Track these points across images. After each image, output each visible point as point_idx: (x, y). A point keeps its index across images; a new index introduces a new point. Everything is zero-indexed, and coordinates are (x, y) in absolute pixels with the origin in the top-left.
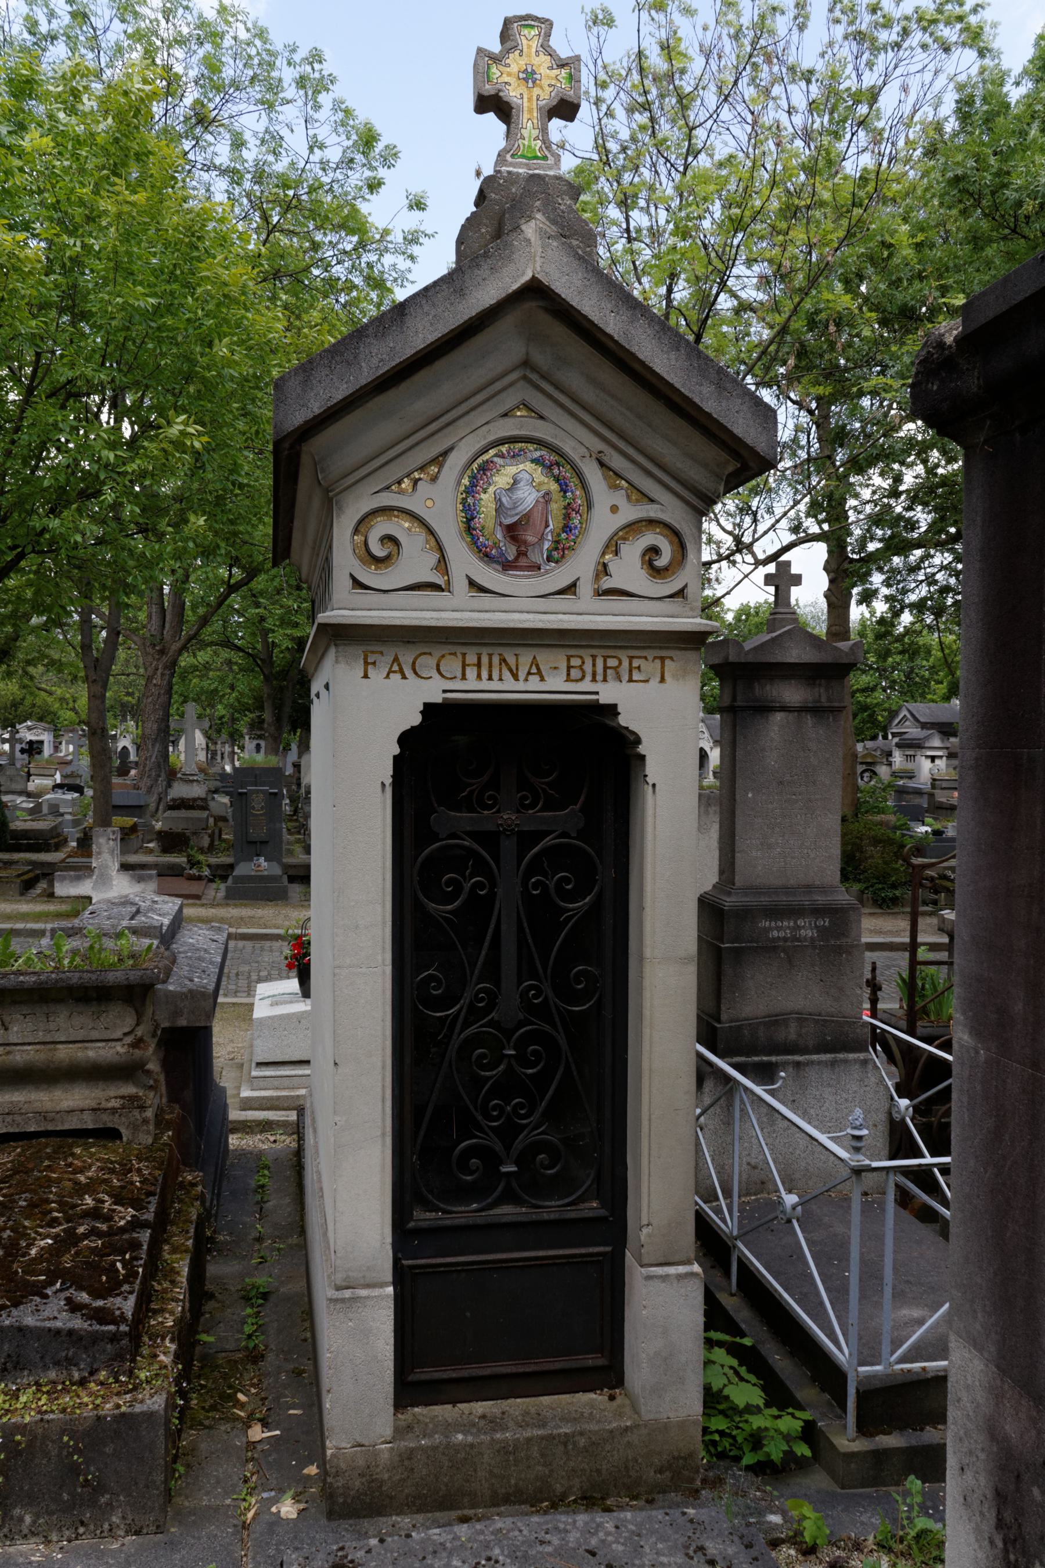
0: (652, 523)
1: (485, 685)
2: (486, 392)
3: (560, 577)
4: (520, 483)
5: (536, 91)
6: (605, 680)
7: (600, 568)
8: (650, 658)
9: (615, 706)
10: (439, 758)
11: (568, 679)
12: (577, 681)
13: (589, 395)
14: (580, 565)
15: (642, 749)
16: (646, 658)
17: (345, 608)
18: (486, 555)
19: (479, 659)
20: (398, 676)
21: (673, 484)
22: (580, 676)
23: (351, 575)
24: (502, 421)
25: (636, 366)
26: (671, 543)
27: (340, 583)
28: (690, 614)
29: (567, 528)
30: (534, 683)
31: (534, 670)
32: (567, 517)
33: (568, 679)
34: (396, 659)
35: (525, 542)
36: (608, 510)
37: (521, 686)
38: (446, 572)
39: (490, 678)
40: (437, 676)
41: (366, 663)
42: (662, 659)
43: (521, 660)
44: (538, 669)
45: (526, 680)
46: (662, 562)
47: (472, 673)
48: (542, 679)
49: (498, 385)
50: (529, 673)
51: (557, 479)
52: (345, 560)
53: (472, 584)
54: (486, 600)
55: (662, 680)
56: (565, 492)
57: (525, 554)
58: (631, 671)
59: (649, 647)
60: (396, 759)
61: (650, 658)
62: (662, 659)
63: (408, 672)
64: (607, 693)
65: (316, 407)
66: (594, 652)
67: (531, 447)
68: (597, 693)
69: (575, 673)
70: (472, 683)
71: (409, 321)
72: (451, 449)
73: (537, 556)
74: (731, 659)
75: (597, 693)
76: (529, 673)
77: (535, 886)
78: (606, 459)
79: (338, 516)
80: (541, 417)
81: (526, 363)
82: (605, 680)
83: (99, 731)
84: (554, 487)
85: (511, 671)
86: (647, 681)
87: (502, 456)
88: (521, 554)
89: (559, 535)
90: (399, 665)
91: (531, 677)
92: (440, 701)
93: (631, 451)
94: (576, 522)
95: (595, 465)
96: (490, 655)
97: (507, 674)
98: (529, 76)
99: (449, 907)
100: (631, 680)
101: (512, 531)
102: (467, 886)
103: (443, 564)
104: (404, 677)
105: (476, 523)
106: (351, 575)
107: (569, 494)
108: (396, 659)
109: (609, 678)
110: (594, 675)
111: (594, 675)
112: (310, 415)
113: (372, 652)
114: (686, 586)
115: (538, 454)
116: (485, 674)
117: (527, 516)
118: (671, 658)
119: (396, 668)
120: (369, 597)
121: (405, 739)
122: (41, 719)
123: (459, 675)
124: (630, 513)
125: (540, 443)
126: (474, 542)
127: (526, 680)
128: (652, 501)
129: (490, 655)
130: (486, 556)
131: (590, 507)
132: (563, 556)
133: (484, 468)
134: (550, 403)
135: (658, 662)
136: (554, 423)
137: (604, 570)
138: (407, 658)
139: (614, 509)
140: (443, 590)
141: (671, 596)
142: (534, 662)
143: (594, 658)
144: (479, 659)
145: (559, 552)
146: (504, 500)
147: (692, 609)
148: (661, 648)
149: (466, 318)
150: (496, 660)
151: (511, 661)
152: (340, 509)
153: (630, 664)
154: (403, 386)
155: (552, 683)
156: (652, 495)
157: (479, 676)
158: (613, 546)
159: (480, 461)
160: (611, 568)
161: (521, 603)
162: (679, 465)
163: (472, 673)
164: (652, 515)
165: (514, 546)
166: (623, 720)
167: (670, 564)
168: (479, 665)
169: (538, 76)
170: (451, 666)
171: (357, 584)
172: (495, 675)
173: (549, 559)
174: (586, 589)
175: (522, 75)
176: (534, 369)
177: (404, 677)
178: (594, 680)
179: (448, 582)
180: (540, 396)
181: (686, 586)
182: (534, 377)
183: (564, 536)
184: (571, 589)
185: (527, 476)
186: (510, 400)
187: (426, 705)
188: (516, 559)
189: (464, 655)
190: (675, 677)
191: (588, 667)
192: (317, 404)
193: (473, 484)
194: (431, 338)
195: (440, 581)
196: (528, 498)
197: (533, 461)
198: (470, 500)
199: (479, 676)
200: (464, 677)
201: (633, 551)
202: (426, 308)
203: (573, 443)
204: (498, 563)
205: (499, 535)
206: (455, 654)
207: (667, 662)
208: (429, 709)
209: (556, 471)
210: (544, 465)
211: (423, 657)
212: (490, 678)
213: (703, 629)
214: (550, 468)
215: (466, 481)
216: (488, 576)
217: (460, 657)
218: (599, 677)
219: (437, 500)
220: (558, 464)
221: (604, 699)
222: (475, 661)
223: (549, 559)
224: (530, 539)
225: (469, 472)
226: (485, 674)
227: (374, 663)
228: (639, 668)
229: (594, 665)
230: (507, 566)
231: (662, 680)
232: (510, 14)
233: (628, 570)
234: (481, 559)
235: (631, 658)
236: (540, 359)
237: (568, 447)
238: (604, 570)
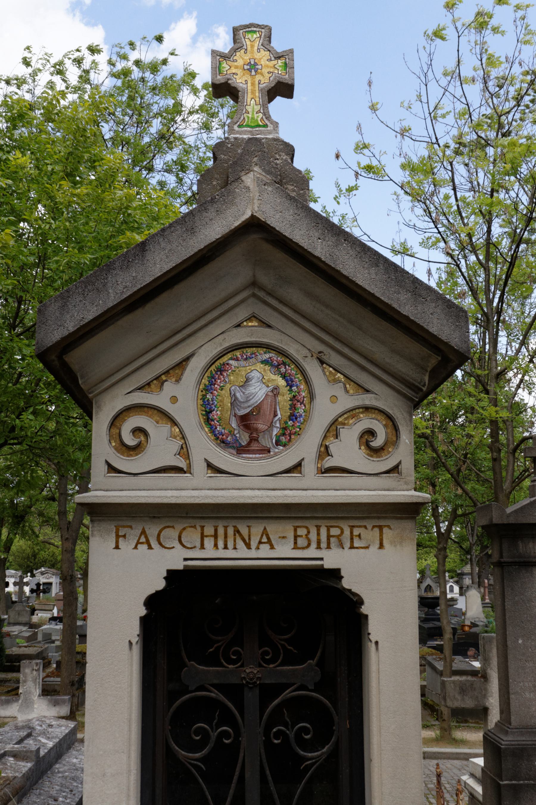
0: (367, 409)
2: (221, 309)
3: (286, 458)
4: (257, 383)
5: (258, 77)
6: (329, 547)
7: (323, 449)
8: (369, 527)
9: (338, 571)
10: (181, 617)
11: (296, 547)
12: (303, 548)
13: (306, 305)
14: (306, 447)
15: (364, 610)
16: (365, 527)
17: (103, 490)
18: (223, 442)
19: (216, 531)
20: (145, 546)
21: (385, 377)
22: (306, 544)
23: (107, 462)
24: (235, 331)
25: (344, 281)
26: (385, 426)
27: (98, 469)
28: (405, 487)
29: (293, 417)
30: (265, 551)
31: (265, 540)
32: (293, 407)
33: (296, 547)
34: (143, 532)
35: (256, 430)
36: (330, 398)
37: (253, 553)
38: (187, 457)
39: (226, 547)
41: (118, 536)
42: (381, 528)
43: (253, 530)
45: (258, 548)
46: (378, 442)
47: (209, 543)
48: (272, 547)
49: (232, 303)
50: (260, 542)
51: (284, 377)
52: (102, 449)
53: (210, 466)
54: (222, 480)
55: (381, 546)
56: (291, 387)
57: (257, 440)
58: (352, 539)
59: (368, 518)
60: (144, 620)
61: (369, 527)
62: (381, 528)
63: (154, 543)
64: (331, 559)
65: (71, 326)
66: (318, 522)
67: (261, 351)
68: (322, 559)
69: (301, 542)
70: (209, 551)
71: (149, 256)
72: (192, 355)
73: (266, 441)
74: (495, 521)
75: (322, 559)
76: (260, 542)
77: (277, 735)
78: (325, 358)
79: (97, 413)
80: (269, 326)
81: (254, 284)
82: (329, 547)
83: (69, 578)
84: (282, 382)
85: (244, 540)
86: (367, 547)
87: (237, 359)
88: (252, 439)
89: (286, 423)
90: (146, 537)
91: (262, 546)
92: (180, 567)
93: (346, 351)
94: (301, 411)
95: (316, 363)
96: (226, 528)
97: (240, 544)
98: (252, 67)
99: (197, 755)
100: (352, 547)
101: (245, 421)
102: (214, 735)
103: (184, 451)
104: (150, 547)
105: (216, 414)
106: (107, 462)
107: (294, 388)
108: (143, 532)
109: (332, 545)
110: (319, 542)
111: (319, 542)
112: (66, 333)
113: (124, 527)
114: (400, 463)
116: (221, 544)
117: (258, 408)
118: (389, 527)
119: (143, 539)
120: (116, 480)
121: (151, 602)
122: (53, 566)
123: (198, 544)
125: (268, 347)
126: (213, 430)
127: (258, 548)
128: (367, 391)
129: (226, 528)
130: (222, 442)
131: (312, 396)
132: (290, 441)
133: (220, 370)
134: (275, 314)
135: (377, 530)
136: (280, 331)
137: (325, 452)
138: (152, 530)
139: (334, 399)
140: (185, 472)
141: (388, 472)
142: (265, 532)
143: (318, 527)
144: (216, 531)
145: (286, 438)
146: (238, 395)
147: (406, 483)
148: (379, 518)
149: (196, 250)
150: (231, 531)
151: (244, 531)
152: (99, 407)
153: (352, 533)
154: (149, 306)
155: (280, 550)
156: (366, 386)
157: (216, 545)
158: (333, 429)
159: (217, 364)
160: (333, 449)
161: (253, 482)
162: (387, 360)
163: (209, 543)
164: (368, 403)
165: (247, 433)
166: (346, 584)
167: (386, 443)
168: (216, 536)
169: (260, 67)
170: (192, 537)
171: (112, 469)
172: (230, 544)
173: (278, 443)
174: (310, 468)
175: (246, 67)
176: (262, 288)
177: (150, 547)
178: (319, 547)
179: (189, 466)
180: (270, 311)
181: (400, 463)
182: (261, 294)
183: (290, 423)
184: (297, 468)
185: (258, 375)
186: (242, 313)
187: (168, 571)
188: (249, 444)
189: (202, 527)
190: (393, 543)
191: (313, 536)
192: (72, 324)
193: (212, 384)
194: (167, 267)
195: (182, 463)
196: (258, 392)
197: (262, 362)
198: (209, 396)
199: (216, 545)
200: (202, 547)
201: (350, 435)
202: (163, 245)
203: (296, 346)
204: (233, 448)
205: (234, 425)
206: (194, 527)
207: (385, 530)
208: (172, 576)
209: (283, 370)
210: (272, 365)
211: (167, 530)
212: (226, 547)
213: (415, 500)
214: (277, 367)
215: (205, 381)
216: (224, 459)
217: (199, 529)
218: (324, 545)
219: (181, 397)
220: (284, 364)
221: (328, 564)
222: (212, 532)
223: (278, 443)
224: (261, 426)
226: (221, 544)
227: (124, 536)
228: (359, 536)
229: (318, 534)
231: (381, 546)
232: (237, 24)
233: (347, 450)
234: (219, 445)
235: (352, 527)
236: (264, 279)
237: (292, 349)
238: (325, 452)
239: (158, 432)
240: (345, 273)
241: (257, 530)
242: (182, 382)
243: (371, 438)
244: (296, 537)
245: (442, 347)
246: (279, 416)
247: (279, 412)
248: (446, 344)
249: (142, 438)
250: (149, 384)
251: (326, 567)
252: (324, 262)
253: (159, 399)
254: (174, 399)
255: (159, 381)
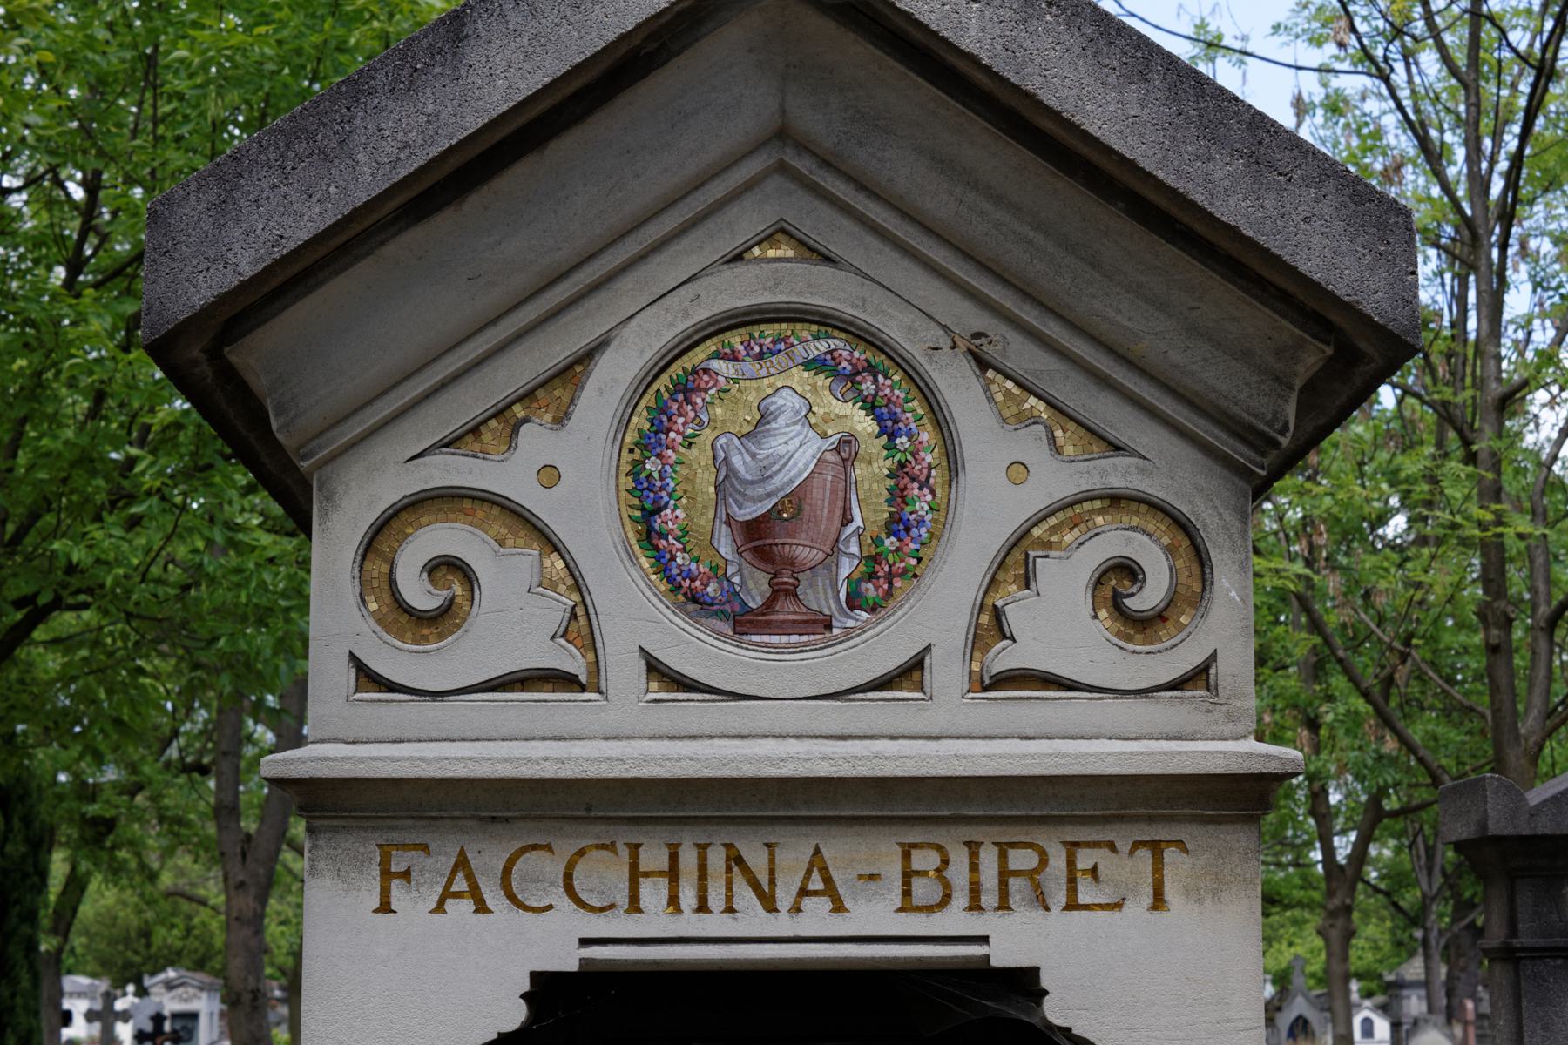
0: (1115, 500)
1: (690, 924)
2: (683, 209)
3: (883, 646)
4: (794, 425)
6: (1004, 906)
7: (985, 619)
8: (1124, 846)
9: (1035, 971)
12: (929, 909)
13: (938, 199)
14: (936, 613)
16: (1112, 846)
17: (347, 740)
18: (693, 598)
19: (674, 858)
20: (467, 905)
21: (1167, 405)
22: (937, 897)
23: (353, 657)
24: (727, 273)
25: (1047, 124)
26: (1170, 551)
27: (327, 676)
28: (1228, 728)
29: (898, 525)
30: (817, 917)
31: (816, 884)
32: (898, 496)
34: (462, 864)
35: (791, 563)
36: (1005, 471)
37: (782, 924)
38: (590, 644)
39: (703, 907)
40: (566, 904)
41: (387, 875)
42: (1156, 848)
43: (783, 858)
44: (828, 880)
45: (796, 909)
46: (1147, 599)
47: (653, 893)
48: (839, 907)
49: (717, 190)
50: (804, 892)
51: (871, 407)
52: (338, 621)
53: (655, 669)
54: (691, 711)
55: (1158, 902)
56: (892, 436)
57: (792, 593)
58: (1072, 881)
59: (1120, 819)
61: (1124, 846)
62: (1156, 848)
63: (493, 896)
64: (1011, 940)
65: (246, 262)
66: (973, 833)
67: (804, 331)
68: (984, 940)
69: (924, 890)
70: (655, 919)
71: (473, 53)
72: (601, 345)
73: (819, 597)
74: (1494, 829)
75: (984, 940)
76: (804, 892)
78: (991, 352)
79: (324, 515)
80: (828, 260)
81: (782, 135)
82: (1004, 906)
83: (247, 998)
84: (864, 424)
85: (755, 886)
86: (1117, 906)
87: (733, 357)
88: (779, 592)
89: (877, 541)
90: (470, 877)
91: (807, 903)
92: (573, 966)
93: (1053, 329)
94: (922, 507)
95: (966, 367)
96: (702, 849)
97: (745, 896)
100: (1072, 906)
101: (759, 538)
103: (580, 626)
104: (481, 907)
105: (672, 518)
106: (353, 657)
107: (902, 441)
108: (462, 864)
109: (1014, 900)
110: (975, 891)
111: (975, 891)
112: (232, 281)
113: (404, 847)
114: (1213, 657)
115: (822, 346)
116: (688, 897)
117: (796, 499)
118: (1180, 844)
119: (460, 884)
120: (383, 710)
122: (200, 965)
123: (622, 898)
124: (1056, 480)
125: (825, 321)
126: (663, 564)
127: (796, 909)
128: (1117, 448)
129: (702, 849)
130: (691, 599)
131: (953, 464)
132: (889, 594)
133: (685, 390)
134: (846, 223)
135: (1145, 855)
136: (858, 272)
137: (992, 626)
138: (488, 858)
139: (1018, 470)
140: (583, 689)
141: (1176, 685)
143: (973, 847)
144: (674, 858)
145: (881, 583)
146: (737, 461)
147: (1232, 718)
148: (1150, 819)
149: (611, 36)
150: (717, 859)
151: (757, 859)
152: (329, 497)
153: (1071, 863)
154: (474, 200)
155: (863, 915)
156: (1113, 434)
157: (674, 901)
158: (1017, 560)
159: (676, 369)
160: (1015, 618)
161: (781, 716)
162: (1175, 356)
163: (653, 893)
164: (1117, 482)
165: (763, 575)
166: (1055, 1011)
167: (1172, 601)
168: (673, 874)
170: (604, 875)
171: (368, 678)
172: (716, 899)
173: (854, 602)
174: (947, 673)
176: (804, 147)
177: (481, 907)
178: (975, 906)
179: (595, 668)
180: (826, 212)
181: (1213, 657)
182: (803, 164)
183: (890, 543)
184: (910, 673)
185: (797, 402)
186: (747, 221)
187: (536, 977)
188: (769, 604)
189: (635, 848)
190: (1192, 892)
191: (959, 874)
192: (250, 255)
193: (660, 427)
194: (527, 86)
195: (575, 664)
196: (795, 452)
197: (808, 365)
198: (652, 466)
199: (674, 901)
200: (634, 906)
201: (1067, 577)
202: (514, 20)
203: (909, 317)
204: (724, 616)
205: (726, 548)
206: (611, 847)
207: (1170, 855)
208: (546, 990)
209: (868, 387)
210: (835, 373)
211: (532, 856)
212: (703, 907)
213: (1256, 768)
214: (852, 378)
215: (640, 421)
216: (697, 648)
217: (624, 853)
218: (989, 899)
219: (570, 467)
220: (871, 369)
221: (1002, 955)
222: (664, 864)
223: (854, 602)
224: (805, 553)
225: (648, 399)
226: (688, 897)
227: (406, 875)
228: (1094, 871)
229: (974, 868)
230: (745, 623)
231: (1158, 902)
233: (1057, 622)
234: (680, 607)
235: (1072, 847)
236: (810, 120)
237: (895, 327)
238: (992, 626)
239: (504, 570)
240: (1051, 100)
241: (794, 854)
242: (572, 423)
243: (1126, 586)
244: (908, 876)
245: (1335, 317)
246: (858, 522)
247: (856, 512)
248: (1349, 309)
249: (458, 589)
250: (475, 431)
251: (995, 962)
252: (987, 70)
253: (506, 475)
254: (549, 475)
255: (504, 421)
